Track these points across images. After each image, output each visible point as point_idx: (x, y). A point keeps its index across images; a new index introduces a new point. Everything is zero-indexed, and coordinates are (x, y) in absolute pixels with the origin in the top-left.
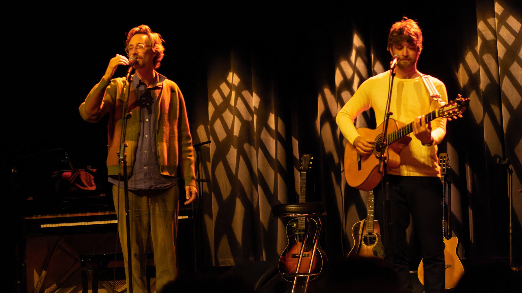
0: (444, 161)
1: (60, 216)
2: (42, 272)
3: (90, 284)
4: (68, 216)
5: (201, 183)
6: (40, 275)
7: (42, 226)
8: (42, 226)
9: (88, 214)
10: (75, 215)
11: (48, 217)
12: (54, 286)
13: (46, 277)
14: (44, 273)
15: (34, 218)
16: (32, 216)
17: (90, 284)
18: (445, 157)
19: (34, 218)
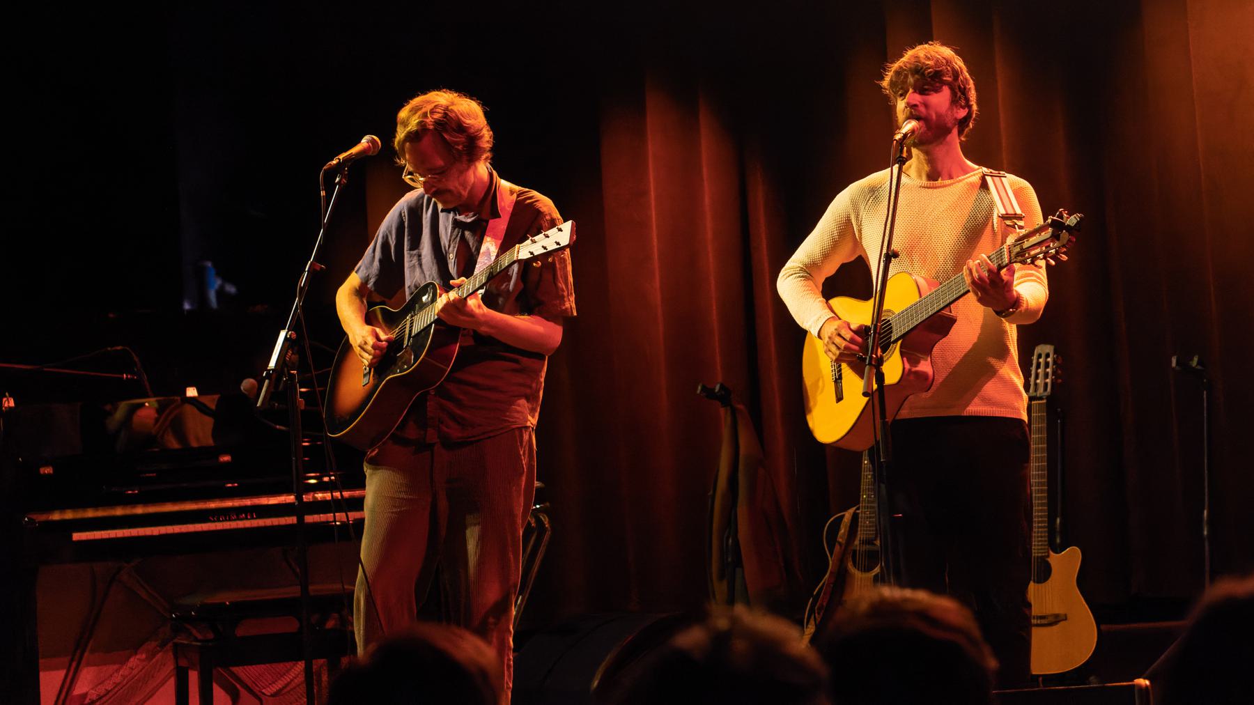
1: (119, 512)
3: (193, 677)
4: (139, 510)
7: (76, 536)
8: (76, 536)
11: (90, 514)
15: (56, 516)
17: (193, 677)
18: (1048, 356)
19: (56, 516)
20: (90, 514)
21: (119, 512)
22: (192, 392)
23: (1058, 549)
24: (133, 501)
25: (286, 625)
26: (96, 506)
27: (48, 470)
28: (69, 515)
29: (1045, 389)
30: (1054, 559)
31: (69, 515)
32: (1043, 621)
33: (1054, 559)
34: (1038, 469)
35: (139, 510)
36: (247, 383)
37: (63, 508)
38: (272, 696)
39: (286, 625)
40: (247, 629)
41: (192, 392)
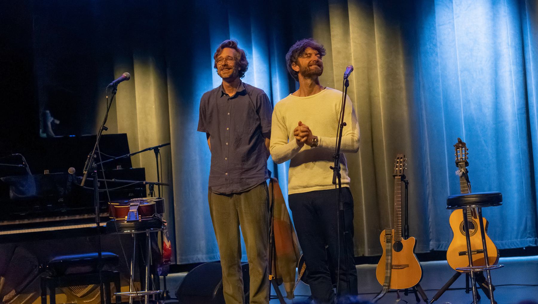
0: (401, 162)
1: (17, 222)
4: (26, 222)
5: (161, 186)
9: (46, 220)
12: (13, 292)
18: (401, 158)
21: (17, 222)
22: (46, 172)
23: (406, 237)
24: (23, 218)
26: (8, 220)
30: (403, 241)
32: (401, 267)
33: (403, 241)
34: (398, 205)
35: (26, 222)
36: (71, 170)
38: (81, 297)
41: (46, 172)
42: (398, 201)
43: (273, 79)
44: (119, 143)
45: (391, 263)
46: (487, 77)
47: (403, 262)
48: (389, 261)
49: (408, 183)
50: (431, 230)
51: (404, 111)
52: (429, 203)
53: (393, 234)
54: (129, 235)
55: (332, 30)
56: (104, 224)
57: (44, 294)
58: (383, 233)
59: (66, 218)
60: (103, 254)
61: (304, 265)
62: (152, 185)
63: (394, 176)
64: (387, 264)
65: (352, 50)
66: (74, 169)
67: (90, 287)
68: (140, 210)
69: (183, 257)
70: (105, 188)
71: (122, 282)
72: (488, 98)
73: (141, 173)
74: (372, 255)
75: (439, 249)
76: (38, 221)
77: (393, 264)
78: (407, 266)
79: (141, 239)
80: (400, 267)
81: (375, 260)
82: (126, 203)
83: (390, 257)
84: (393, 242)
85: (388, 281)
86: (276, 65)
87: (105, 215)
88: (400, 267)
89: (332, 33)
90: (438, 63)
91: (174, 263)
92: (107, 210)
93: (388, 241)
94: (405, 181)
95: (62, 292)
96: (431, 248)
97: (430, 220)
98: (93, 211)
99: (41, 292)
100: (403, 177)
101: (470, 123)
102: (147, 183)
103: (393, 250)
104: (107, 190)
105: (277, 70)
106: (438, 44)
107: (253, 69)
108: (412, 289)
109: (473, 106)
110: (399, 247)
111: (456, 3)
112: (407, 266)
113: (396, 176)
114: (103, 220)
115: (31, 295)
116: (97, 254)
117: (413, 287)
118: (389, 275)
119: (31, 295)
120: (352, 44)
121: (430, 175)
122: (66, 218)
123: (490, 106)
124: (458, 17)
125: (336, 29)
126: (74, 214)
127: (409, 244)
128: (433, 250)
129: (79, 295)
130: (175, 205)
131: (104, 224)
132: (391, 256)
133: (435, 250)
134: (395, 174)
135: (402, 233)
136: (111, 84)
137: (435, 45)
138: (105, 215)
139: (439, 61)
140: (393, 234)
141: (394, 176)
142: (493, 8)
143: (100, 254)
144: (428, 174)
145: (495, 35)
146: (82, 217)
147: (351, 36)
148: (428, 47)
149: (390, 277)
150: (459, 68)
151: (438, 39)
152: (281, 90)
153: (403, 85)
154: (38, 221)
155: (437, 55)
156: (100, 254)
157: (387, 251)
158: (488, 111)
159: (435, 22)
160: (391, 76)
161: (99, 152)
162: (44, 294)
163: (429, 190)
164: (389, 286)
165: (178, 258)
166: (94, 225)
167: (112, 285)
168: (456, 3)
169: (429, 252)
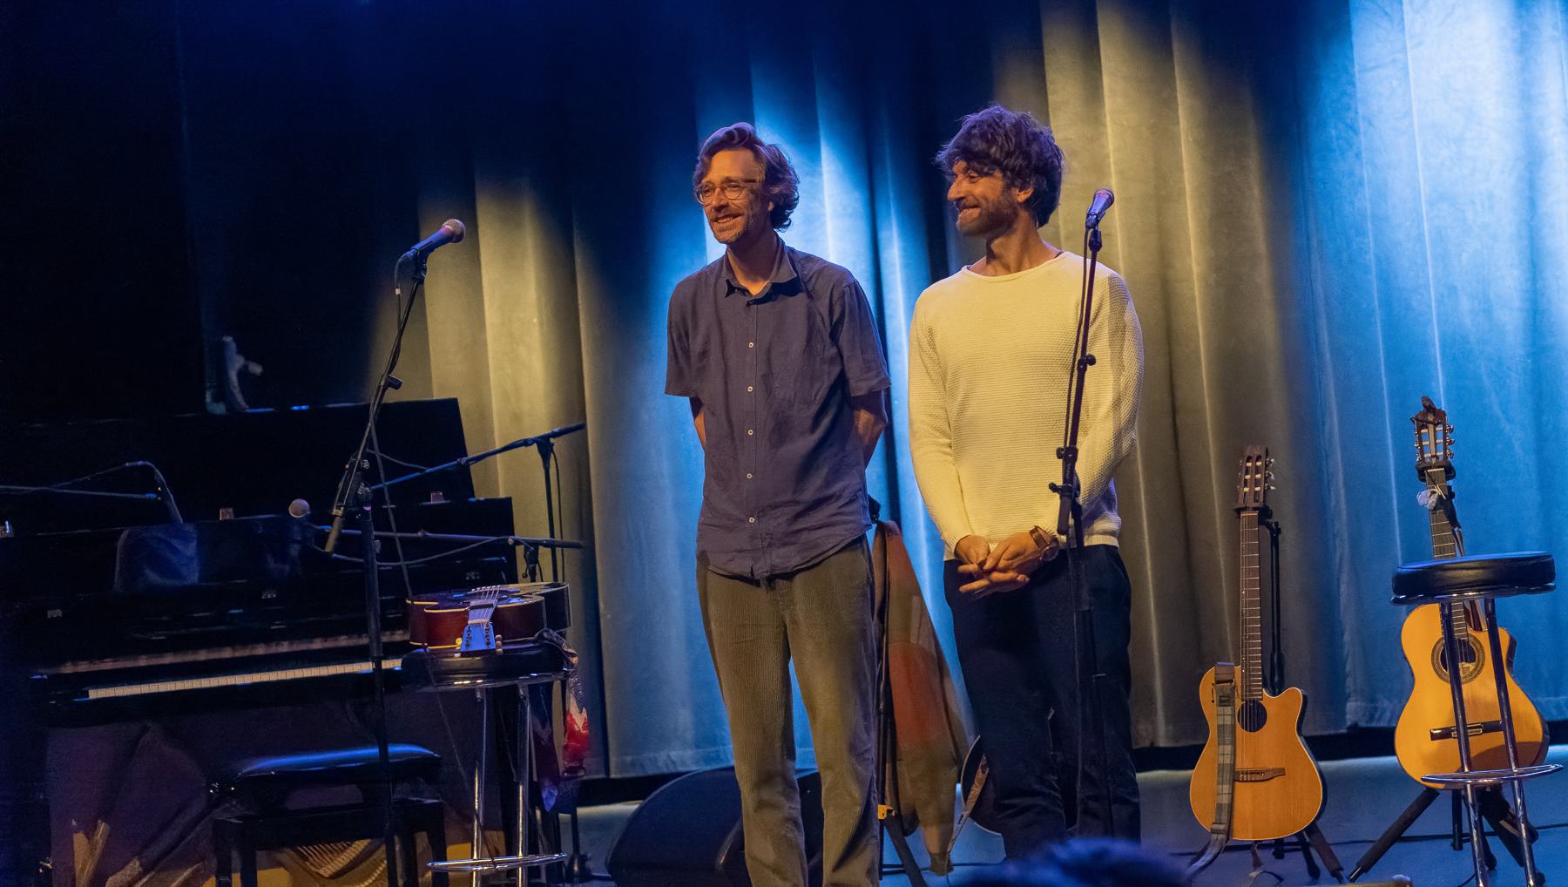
0: (1257, 470)
2: (96, 827)
3: (235, 856)
4: (168, 659)
5: (558, 550)
6: (89, 835)
7: (94, 694)
8: (94, 694)
9: (227, 653)
10: (189, 657)
11: (108, 665)
12: (135, 866)
13: (110, 837)
14: (102, 827)
15: (68, 669)
16: (62, 662)
17: (235, 856)
18: (1259, 458)
20: (108, 665)
22: (226, 514)
23: (1276, 688)
24: (160, 649)
25: (349, 794)
27: (58, 613)
28: (83, 667)
29: (1256, 501)
30: (1267, 698)
31: (83, 667)
33: (1267, 698)
34: (1251, 594)
35: (168, 659)
37: (75, 659)
39: (349, 794)
40: (300, 800)
41: (226, 514)
42: (1251, 583)
43: (883, 235)
44: (437, 427)
45: (1234, 765)
46: (1505, 220)
47: (1269, 762)
48: (1228, 761)
49: (1279, 531)
50: (1348, 668)
51: (1265, 324)
52: (1343, 588)
53: (1238, 680)
54: (469, 692)
55: (1050, 87)
56: (395, 664)
57: (223, 871)
58: (1209, 676)
59: (285, 648)
60: (394, 749)
61: (980, 776)
62: (533, 548)
63: (1239, 511)
64: (1221, 768)
65: (1111, 147)
66: (305, 503)
67: (360, 845)
68: (499, 621)
69: (629, 759)
70: (398, 560)
71: (450, 832)
72: (1509, 281)
73: (500, 513)
74: (1182, 744)
75: (1374, 725)
76: (202, 656)
77: (1239, 766)
78: (1281, 772)
79: (504, 702)
80: (1258, 776)
81: (1186, 757)
82: (457, 600)
83: (1228, 748)
84: (1239, 703)
85: (1225, 818)
86: (892, 195)
87: (399, 636)
88: (1258, 776)
89: (1051, 98)
90: (1361, 184)
91: (602, 776)
92: (400, 624)
93: (1225, 701)
94: (1269, 526)
95: (280, 864)
96: (1350, 719)
97: (1347, 638)
98: (359, 628)
99: (214, 863)
100: (1264, 513)
101: (1459, 355)
102: (517, 542)
103: (1238, 726)
104: (402, 563)
105: (893, 211)
106: (1362, 126)
107: (823, 206)
108: (1295, 840)
109: (1465, 304)
110: (1254, 717)
111: (1411, 3)
112: (1281, 772)
113: (1245, 509)
114: (391, 650)
115: (186, 873)
116: (375, 751)
117: (1299, 835)
118: (1225, 800)
119: (186, 873)
120: (1110, 129)
121: (1343, 506)
122: (285, 648)
123: (1517, 304)
124: (1419, 44)
125: (1063, 87)
126: (310, 635)
127: (1284, 707)
128: (1354, 727)
129: (326, 871)
130: (602, 605)
131: (395, 664)
132: (1234, 743)
133: (1363, 724)
134: (1241, 504)
135: (1263, 676)
136: (410, 253)
137: (1352, 128)
138: (399, 636)
139: (1366, 173)
140: (1238, 680)
141: (1239, 511)
142: (1520, 17)
143: (384, 751)
144: (1338, 502)
145: (1526, 95)
146: (330, 644)
147: (1109, 103)
148: (1333, 132)
149: (1231, 806)
150: (1424, 189)
151: (1360, 111)
152: (906, 266)
153: (1261, 245)
154: (202, 656)
155: (1358, 155)
156: (384, 751)
157: (1221, 728)
158: (1511, 319)
159: (1352, 60)
160: (1224, 219)
161: (378, 454)
162: (223, 871)
163: (1342, 549)
164: (1229, 832)
165: (613, 760)
166: (366, 667)
167: (422, 840)
168: (1411, 3)
169: (1344, 731)
